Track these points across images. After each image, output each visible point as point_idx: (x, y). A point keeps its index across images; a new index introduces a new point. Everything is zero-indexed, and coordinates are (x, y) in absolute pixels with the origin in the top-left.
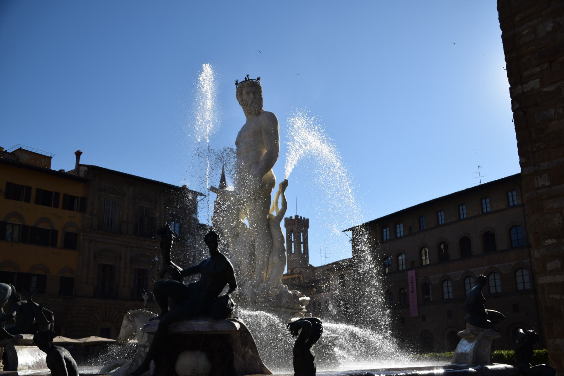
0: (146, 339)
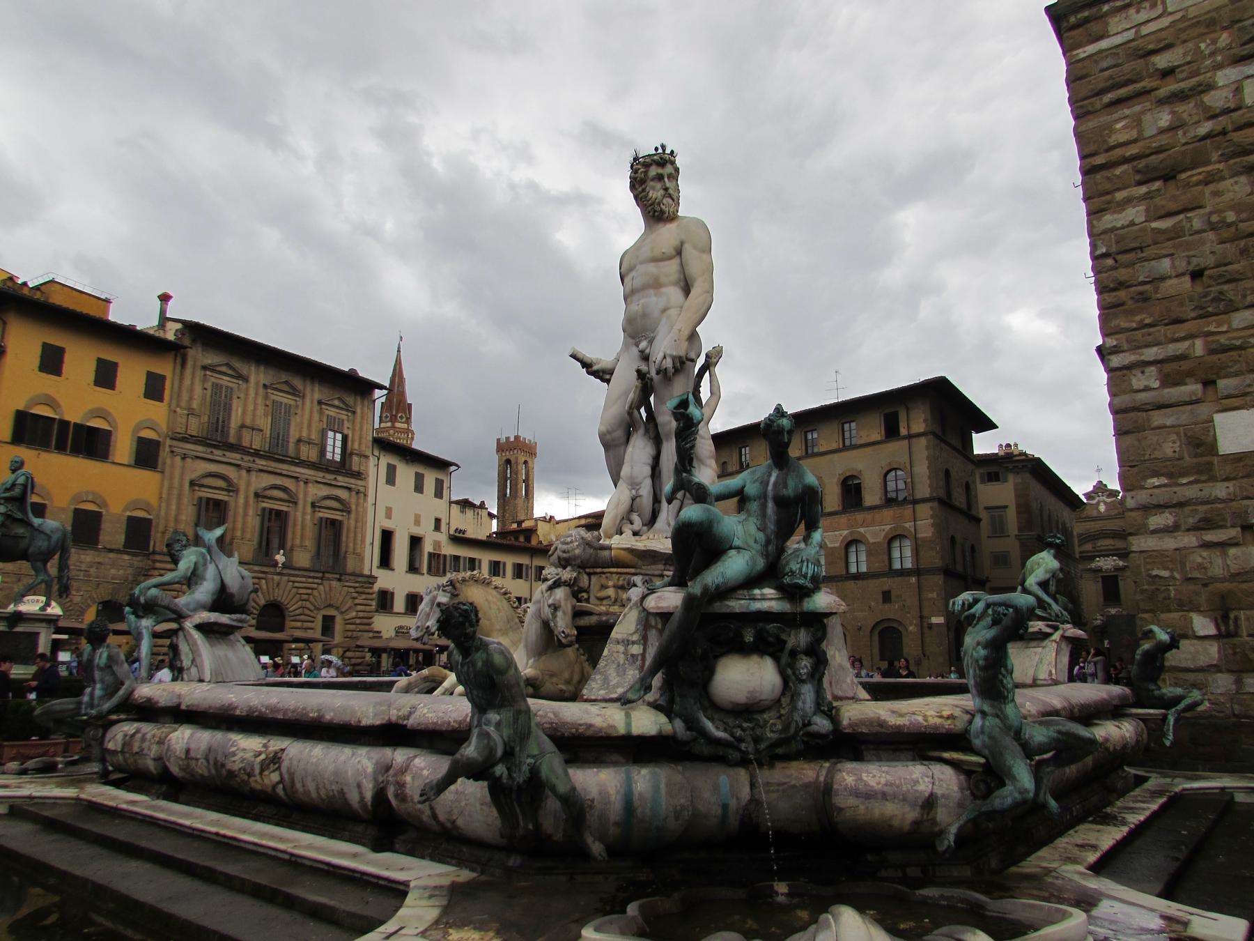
0: (632, 628)
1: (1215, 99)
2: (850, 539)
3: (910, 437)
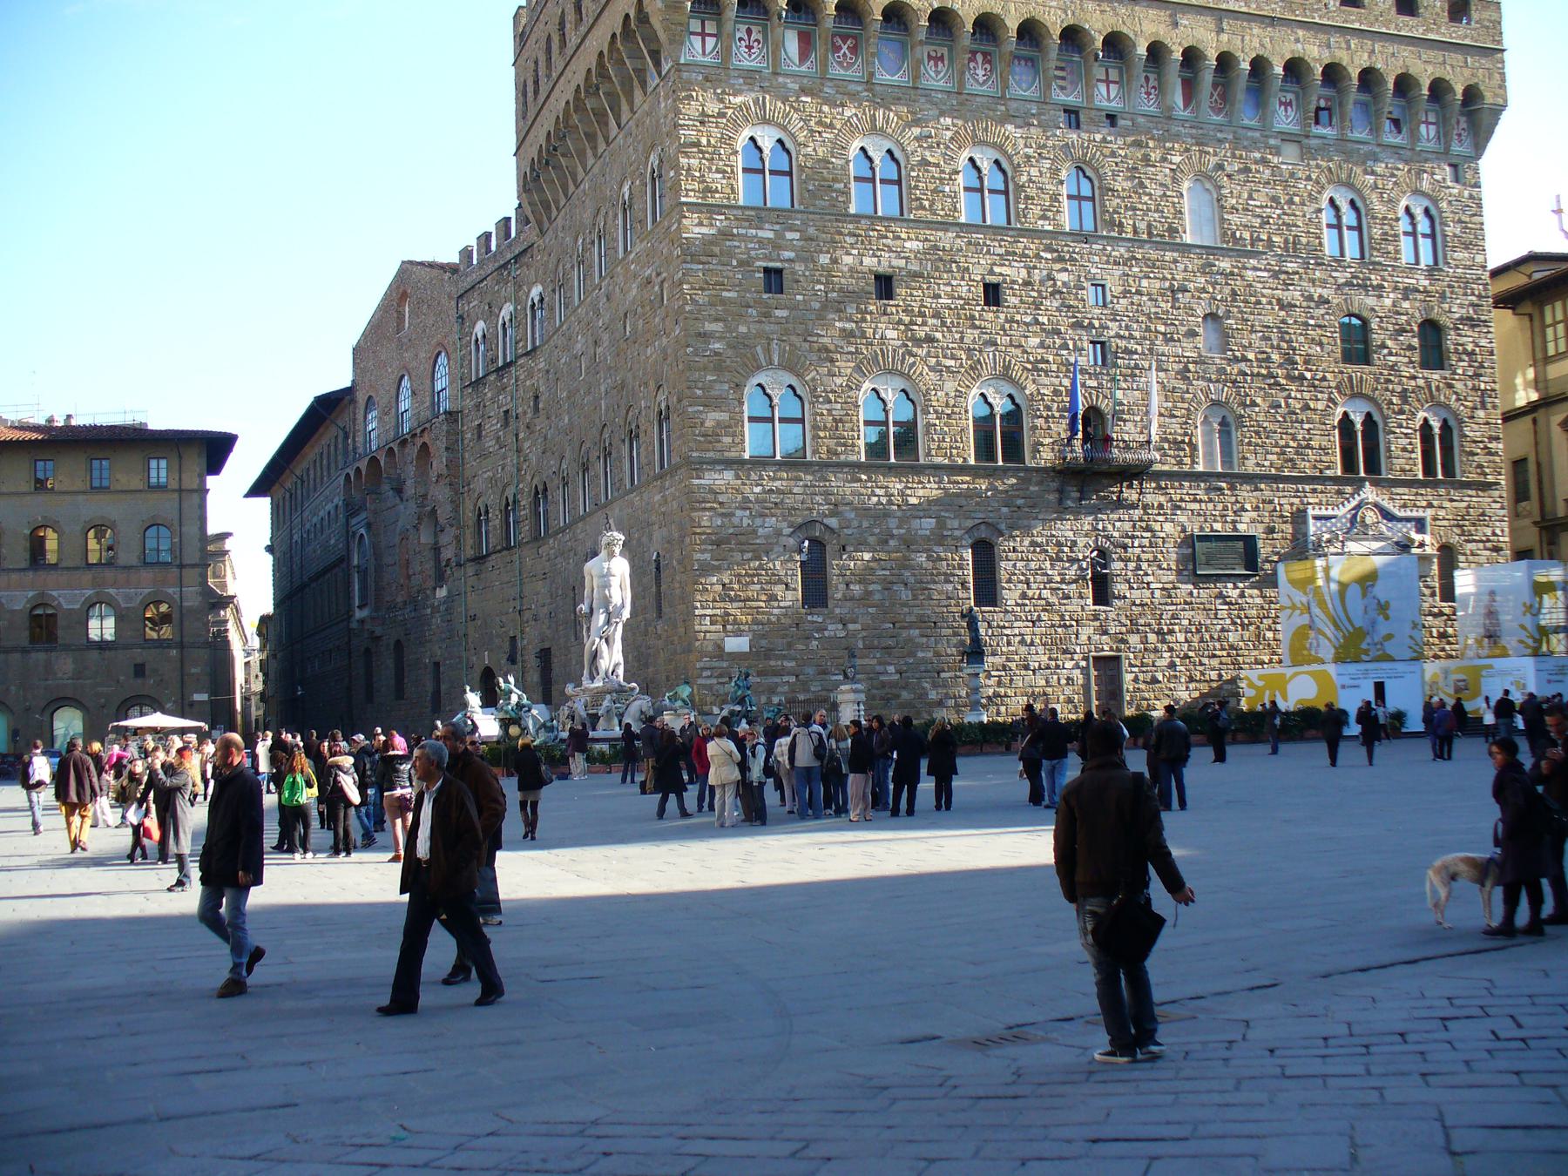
1: (736, 521)
2: (95, 600)
3: (180, 490)
